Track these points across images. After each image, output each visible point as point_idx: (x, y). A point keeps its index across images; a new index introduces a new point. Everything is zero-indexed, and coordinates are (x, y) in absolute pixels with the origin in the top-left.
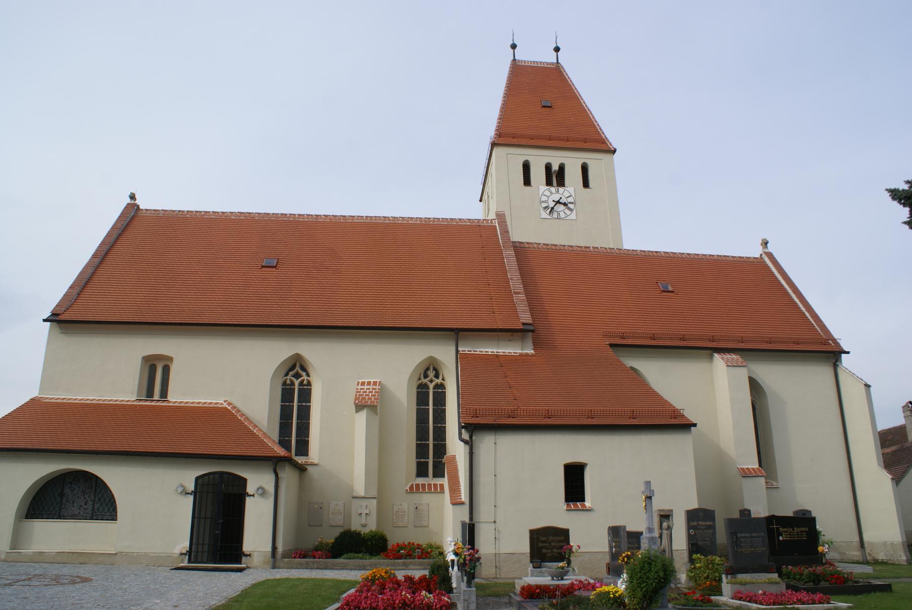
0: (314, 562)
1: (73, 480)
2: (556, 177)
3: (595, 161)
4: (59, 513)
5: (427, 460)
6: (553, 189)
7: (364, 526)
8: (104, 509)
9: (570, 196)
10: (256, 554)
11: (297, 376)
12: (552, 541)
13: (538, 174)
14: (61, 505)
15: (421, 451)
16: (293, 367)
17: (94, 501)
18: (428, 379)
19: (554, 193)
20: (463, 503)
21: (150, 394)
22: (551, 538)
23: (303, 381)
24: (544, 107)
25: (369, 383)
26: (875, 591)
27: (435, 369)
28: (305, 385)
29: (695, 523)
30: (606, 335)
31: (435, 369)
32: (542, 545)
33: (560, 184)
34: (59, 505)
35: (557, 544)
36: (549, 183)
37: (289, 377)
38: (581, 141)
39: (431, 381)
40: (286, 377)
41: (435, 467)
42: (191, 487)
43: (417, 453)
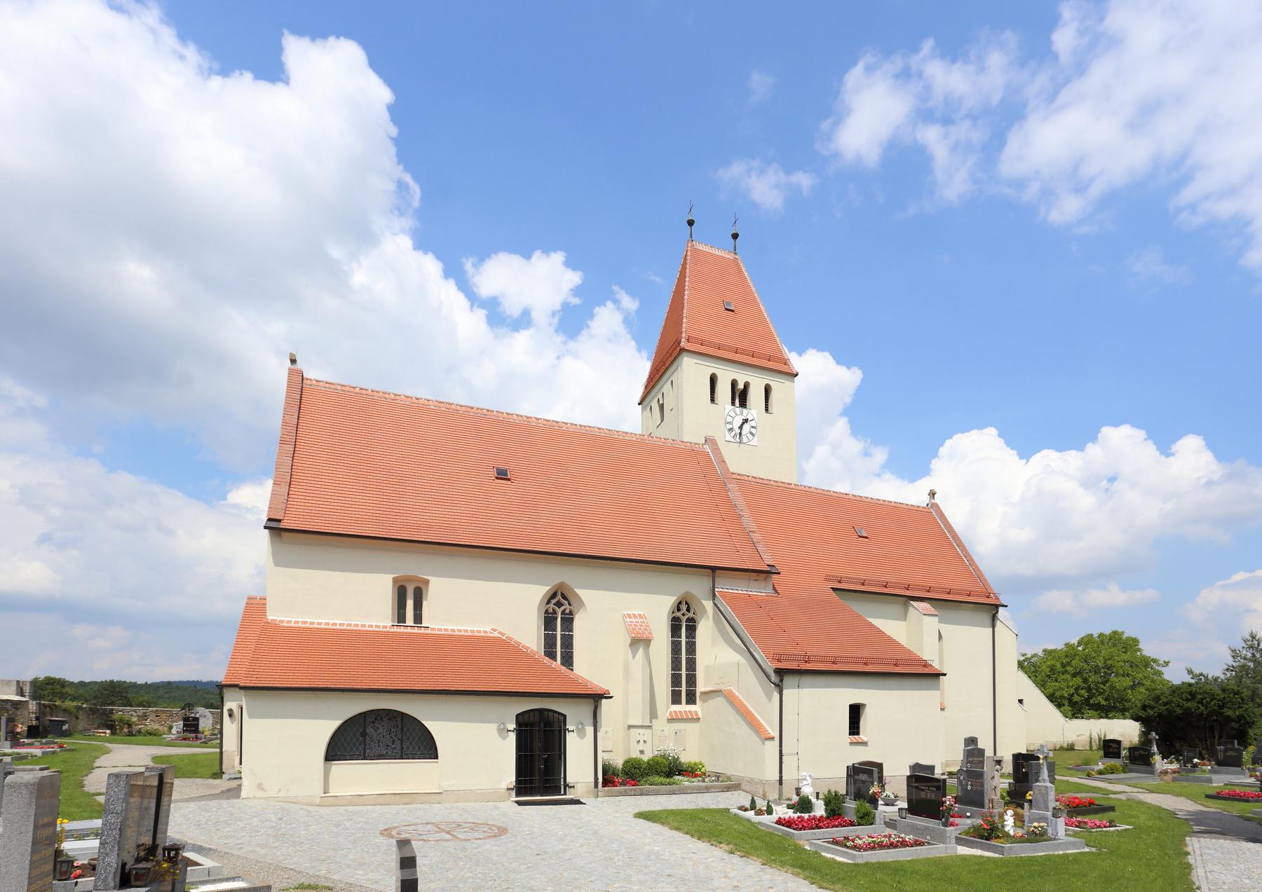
0: (631, 790)
1: (376, 719)
2: (740, 396)
3: (778, 385)
4: (364, 754)
7: (642, 752)
8: (414, 748)
9: (753, 420)
10: (579, 785)
11: (559, 604)
13: (724, 390)
14: (365, 745)
15: (676, 680)
16: (554, 596)
17: (402, 741)
20: (772, 738)
21: (401, 618)
23: (564, 610)
25: (635, 616)
26: (1109, 811)
27: (687, 603)
28: (567, 614)
29: (971, 759)
31: (687, 603)
34: (363, 746)
37: (551, 605)
38: (765, 359)
39: (683, 615)
40: (548, 606)
41: (687, 695)
42: (512, 726)
43: (672, 682)
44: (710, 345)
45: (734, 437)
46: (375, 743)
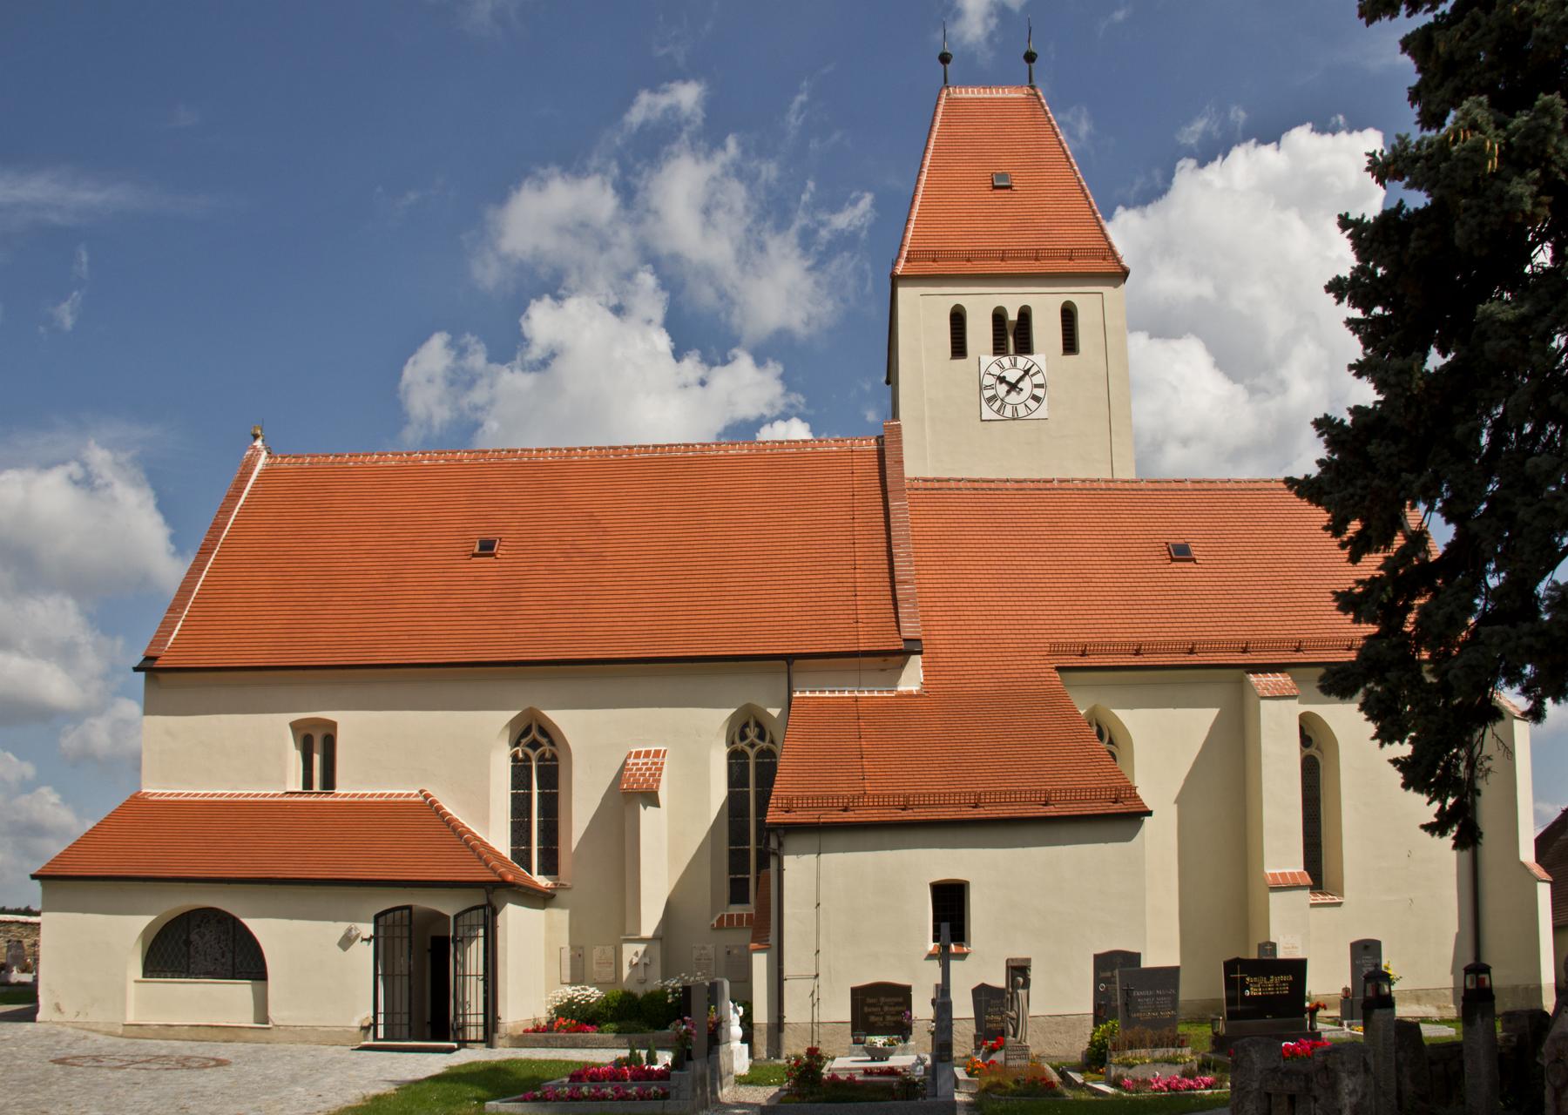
1: (202, 921)
4: (188, 971)
5: (747, 876)
6: (1006, 361)
12: (885, 1003)
13: (980, 332)
14: (189, 958)
17: (234, 953)
18: (747, 742)
19: (1018, 366)
22: (883, 999)
23: (543, 754)
24: (995, 188)
25: (647, 754)
27: (759, 725)
28: (547, 760)
30: (1055, 649)
32: (870, 1010)
33: (1021, 348)
34: (186, 959)
35: (892, 1009)
36: (999, 348)
38: (1063, 258)
44: (952, 256)
45: (998, 411)
46: (200, 955)
